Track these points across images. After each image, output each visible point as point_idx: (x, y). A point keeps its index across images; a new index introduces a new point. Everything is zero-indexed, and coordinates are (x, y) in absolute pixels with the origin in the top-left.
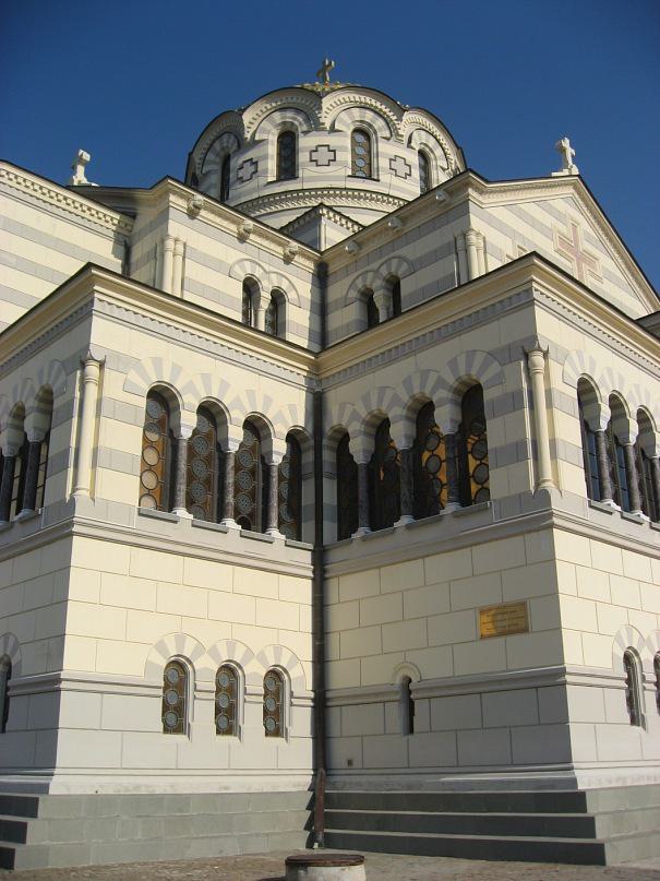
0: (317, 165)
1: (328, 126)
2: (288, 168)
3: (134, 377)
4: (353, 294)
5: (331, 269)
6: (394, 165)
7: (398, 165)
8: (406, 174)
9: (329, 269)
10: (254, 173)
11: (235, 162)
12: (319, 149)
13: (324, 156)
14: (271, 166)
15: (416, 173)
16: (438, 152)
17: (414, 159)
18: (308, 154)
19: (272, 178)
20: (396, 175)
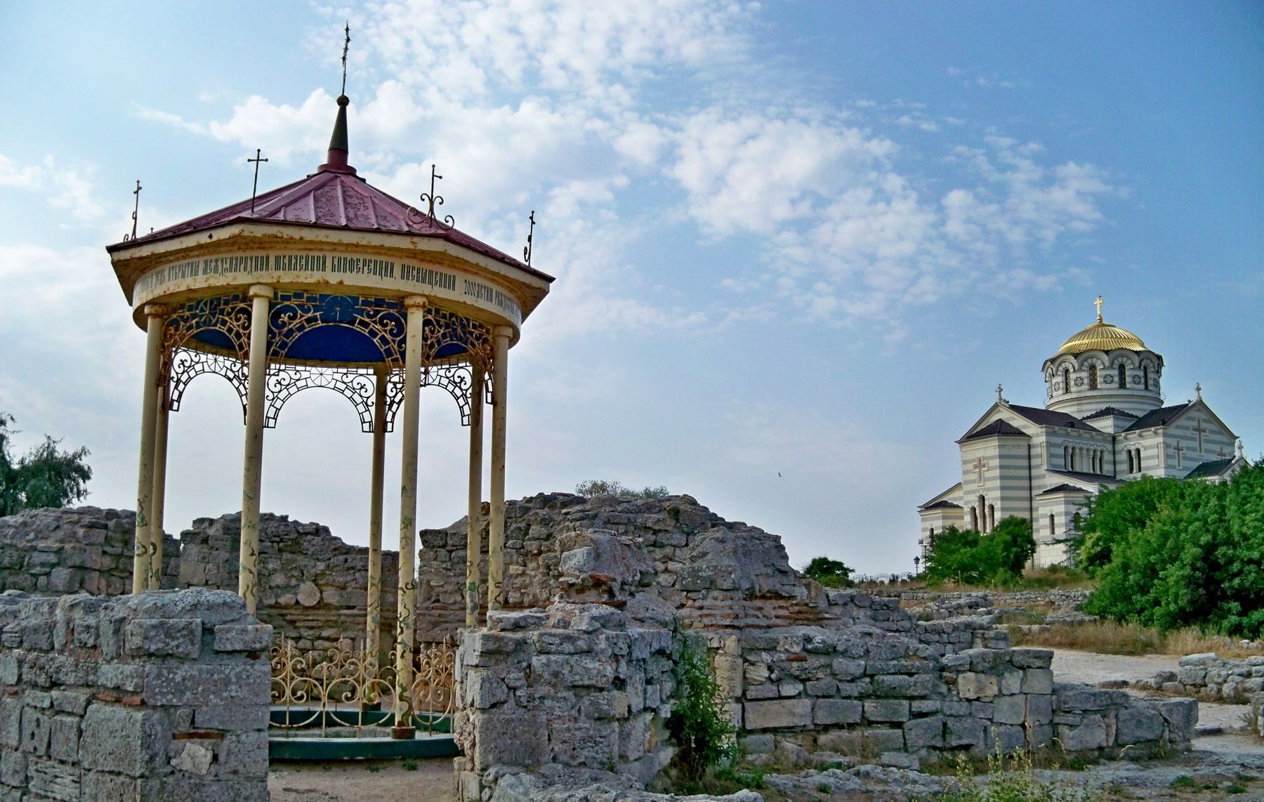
7: (1079, 382)
13: (1057, 387)
15: (1086, 381)
16: (1099, 362)
17: (1085, 375)
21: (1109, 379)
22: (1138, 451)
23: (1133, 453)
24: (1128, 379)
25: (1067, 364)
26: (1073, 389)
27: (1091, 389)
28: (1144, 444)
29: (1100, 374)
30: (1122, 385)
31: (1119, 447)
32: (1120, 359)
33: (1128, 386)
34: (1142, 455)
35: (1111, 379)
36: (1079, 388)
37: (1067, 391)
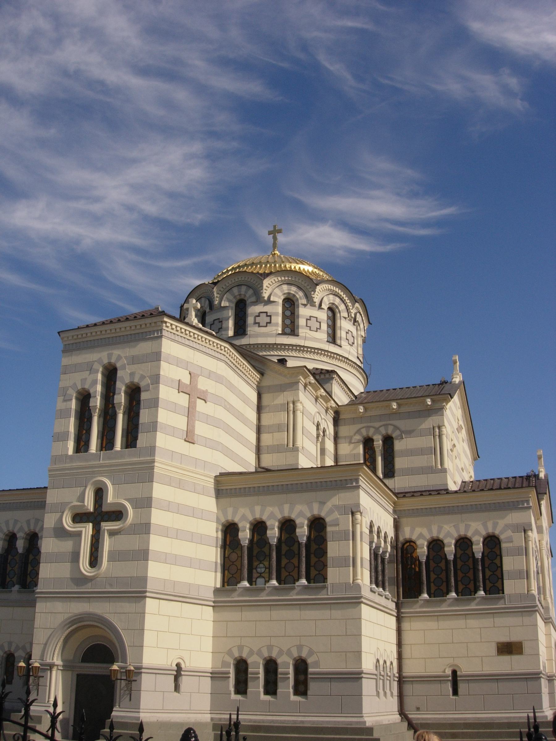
6: (258, 320)
7: (263, 319)
8: (267, 323)
15: (278, 320)
20: (259, 326)
22: (388, 441)
23: (378, 443)
24: (341, 334)
25: (244, 288)
27: (284, 333)
28: (403, 429)
29: (304, 312)
30: (333, 338)
31: (344, 430)
32: (331, 297)
33: (338, 342)
34: (398, 446)
35: (318, 325)
36: (263, 330)
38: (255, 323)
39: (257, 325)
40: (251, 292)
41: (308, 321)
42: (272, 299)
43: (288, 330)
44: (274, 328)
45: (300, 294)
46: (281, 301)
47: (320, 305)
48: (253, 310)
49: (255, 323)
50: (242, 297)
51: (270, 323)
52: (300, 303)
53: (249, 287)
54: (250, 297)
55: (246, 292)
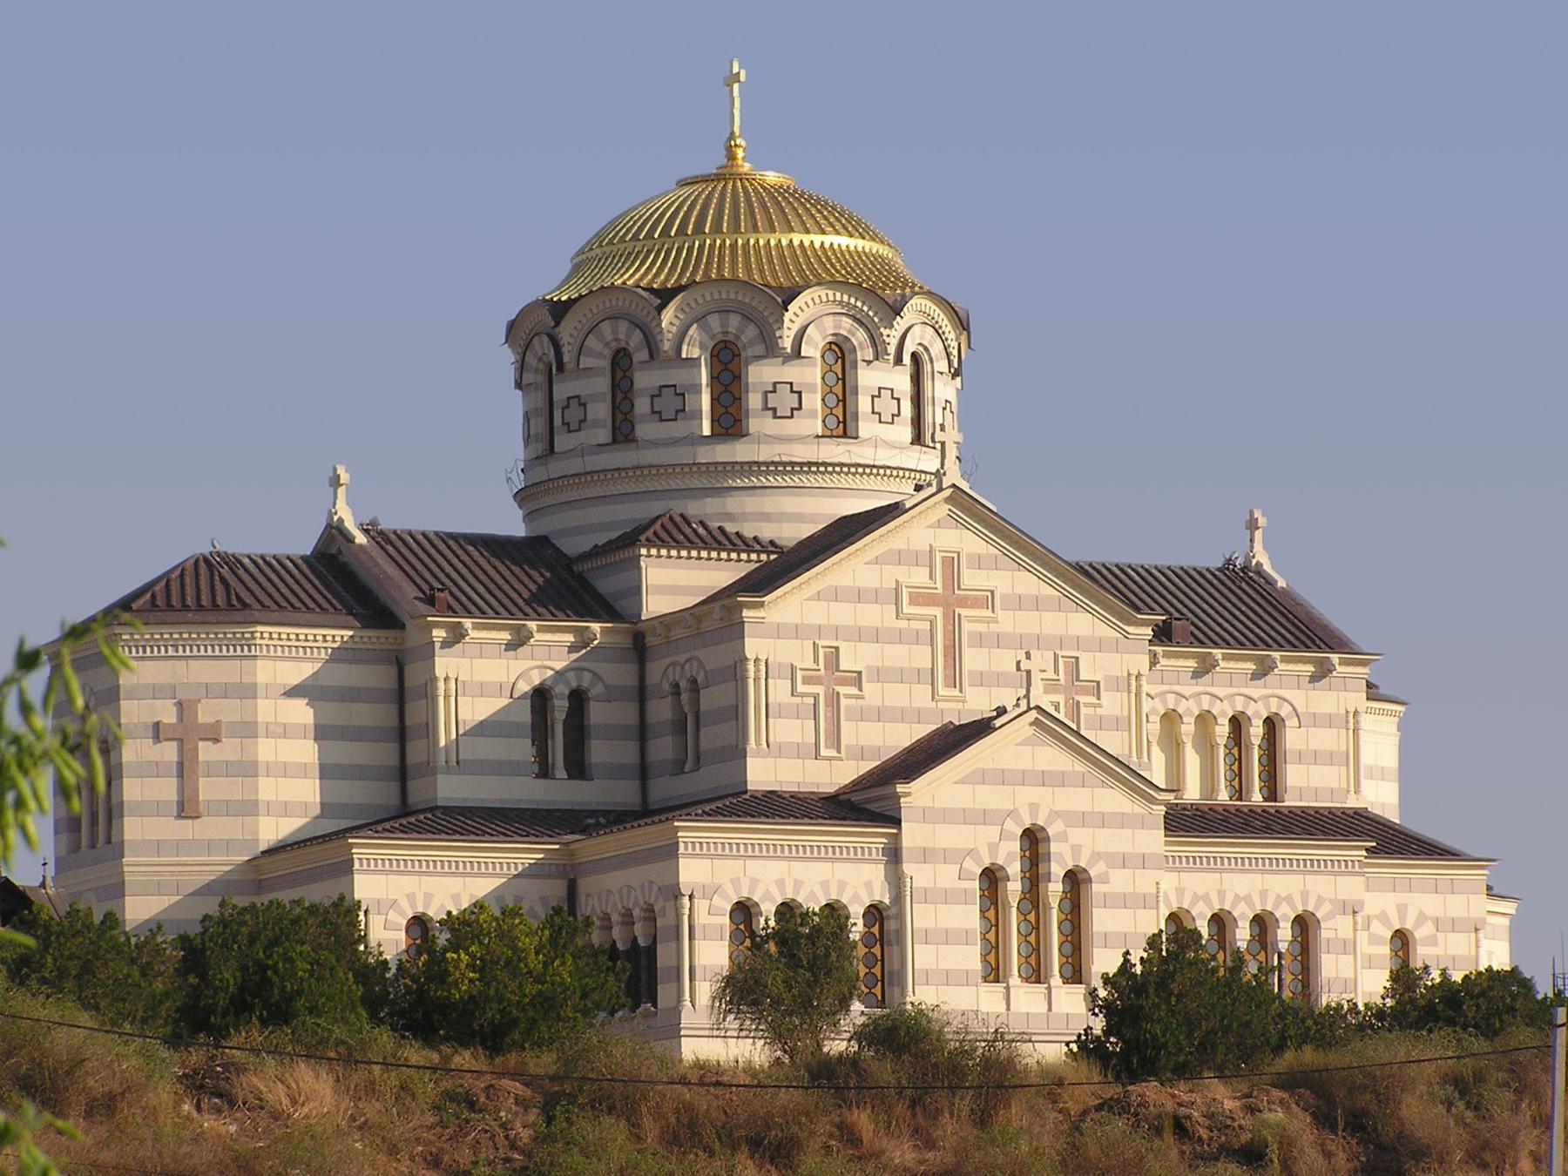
0: (661, 420)
1: (672, 353)
2: (623, 432)
3: (392, 916)
4: (666, 687)
5: (650, 641)
7: (785, 400)
9: (646, 641)
10: (580, 422)
11: (562, 391)
12: (664, 390)
13: (668, 404)
14: (600, 411)
15: (813, 401)
17: (810, 375)
18: (647, 401)
19: (604, 435)
20: (775, 417)
21: (886, 406)
26: (758, 424)
29: (869, 377)
37: (730, 423)
38: (766, 408)
39: (770, 412)
40: (751, 332)
41: (876, 399)
42: (803, 354)
43: (832, 422)
44: (809, 421)
45: (860, 337)
46: (818, 356)
47: (899, 360)
48: (760, 374)
49: (766, 408)
50: (730, 338)
51: (800, 408)
52: (859, 358)
53: (747, 318)
54: (751, 344)
55: (741, 330)
